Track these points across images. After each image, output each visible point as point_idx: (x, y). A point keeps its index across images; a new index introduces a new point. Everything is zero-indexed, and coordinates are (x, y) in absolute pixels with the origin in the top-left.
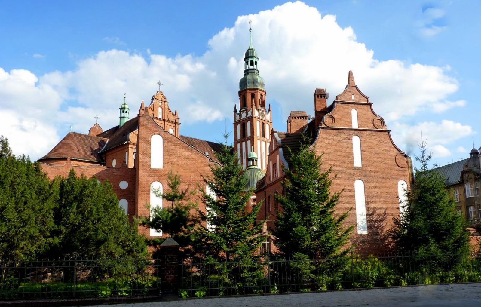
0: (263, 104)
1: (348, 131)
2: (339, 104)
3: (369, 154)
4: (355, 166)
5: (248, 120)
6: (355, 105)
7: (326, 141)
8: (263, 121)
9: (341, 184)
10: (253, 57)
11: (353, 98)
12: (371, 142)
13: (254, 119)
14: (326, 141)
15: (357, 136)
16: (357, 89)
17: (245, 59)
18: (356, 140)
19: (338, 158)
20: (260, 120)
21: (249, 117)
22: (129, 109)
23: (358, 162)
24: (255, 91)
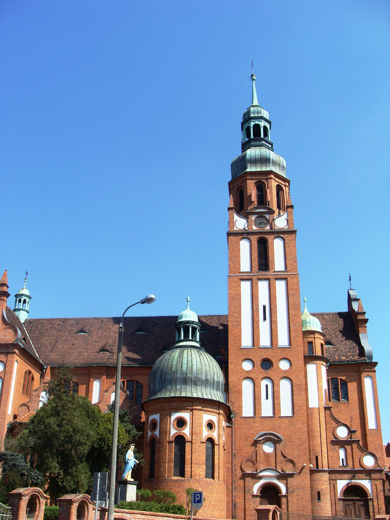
22: (30, 297)
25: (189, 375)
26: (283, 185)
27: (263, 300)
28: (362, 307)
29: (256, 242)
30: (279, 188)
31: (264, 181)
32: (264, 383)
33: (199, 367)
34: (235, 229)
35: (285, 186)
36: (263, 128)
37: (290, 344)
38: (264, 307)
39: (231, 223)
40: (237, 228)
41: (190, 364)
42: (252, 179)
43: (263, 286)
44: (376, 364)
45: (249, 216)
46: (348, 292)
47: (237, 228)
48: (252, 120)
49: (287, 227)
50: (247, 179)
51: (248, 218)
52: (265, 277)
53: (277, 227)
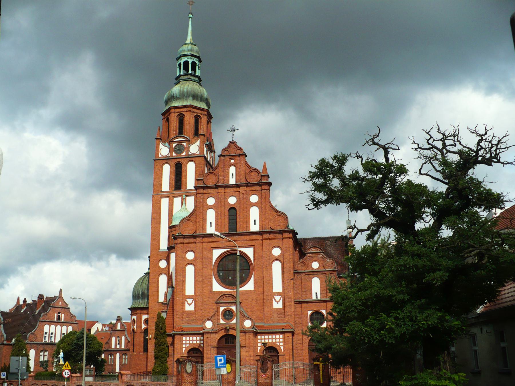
8: (178, 160)
26: (202, 114)
30: (197, 119)
31: (184, 113)
34: (160, 156)
35: (204, 115)
36: (192, 64)
39: (158, 151)
40: (161, 155)
42: (174, 112)
43: (177, 201)
45: (171, 144)
47: (161, 155)
48: (182, 58)
49: (198, 153)
50: (171, 113)
52: (179, 194)
53: (191, 153)
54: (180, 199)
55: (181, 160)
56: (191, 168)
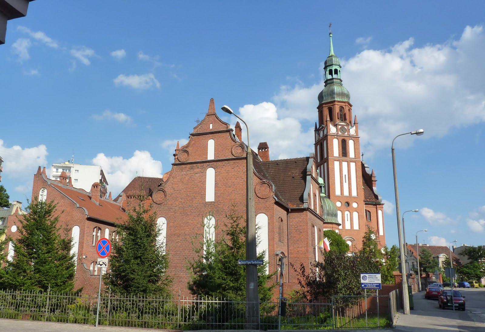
0: (343, 117)
1: (202, 164)
2: (195, 137)
3: (224, 186)
4: (206, 201)
5: (324, 139)
6: (213, 135)
7: (178, 178)
9: (190, 221)
10: (332, 65)
11: (211, 127)
12: (227, 173)
13: (329, 137)
14: (178, 178)
15: (212, 167)
16: (216, 116)
17: (324, 68)
18: (211, 173)
19: (189, 194)
20: (338, 137)
21: (325, 135)
23: (210, 196)
24: (332, 104)
25: (330, 212)
27: (345, 172)
28: (374, 174)
29: (341, 141)
32: (347, 213)
33: (333, 208)
34: (331, 133)
37: (358, 195)
38: (345, 175)
41: (329, 206)
42: (338, 105)
44: (383, 204)
46: (362, 162)
49: (355, 135)
50: (335, 105)
51: (337, 127)
54: (346, 163)
55: (346, 138)
56: (351, 144)
